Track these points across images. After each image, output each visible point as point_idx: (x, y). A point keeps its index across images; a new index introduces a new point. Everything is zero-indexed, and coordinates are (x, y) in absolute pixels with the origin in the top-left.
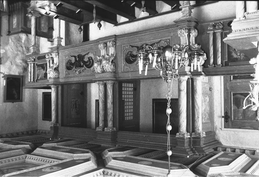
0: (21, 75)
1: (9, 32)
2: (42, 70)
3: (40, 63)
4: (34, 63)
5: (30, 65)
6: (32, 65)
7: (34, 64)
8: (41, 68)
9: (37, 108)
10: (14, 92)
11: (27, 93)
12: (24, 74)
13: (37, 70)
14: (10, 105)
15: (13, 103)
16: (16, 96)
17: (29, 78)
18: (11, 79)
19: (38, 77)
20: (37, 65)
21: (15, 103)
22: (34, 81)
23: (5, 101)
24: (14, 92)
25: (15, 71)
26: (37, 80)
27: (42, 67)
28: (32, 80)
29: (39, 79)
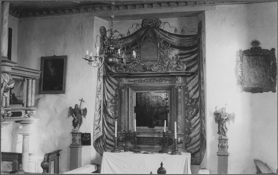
0: (41, 96)
1: (58, 155)
2: (16, 95)
3: (17, 108)
4: (27, 107)
5: (33, 105)
6: (29, 105)
7: (27, 106)
8: (18, 98)
9: (18, 46)
10: (52, 70)
11: (35, 64)
12: (38, 97)
13: (22, 96)
14: (59, 53)
15: (54, 55)
16: (50, 64)
17: (33, 86)
18: (56, 88)
19: (22, 85)
20: (23, 105)
21: (53, 55)
22: (28, 80)
23: (66, 57)
24: (52, 70)
25: (50, 100)
26: (24, 80)
27: (17, 100)
28: (30, 80)
29: (21, 82)
